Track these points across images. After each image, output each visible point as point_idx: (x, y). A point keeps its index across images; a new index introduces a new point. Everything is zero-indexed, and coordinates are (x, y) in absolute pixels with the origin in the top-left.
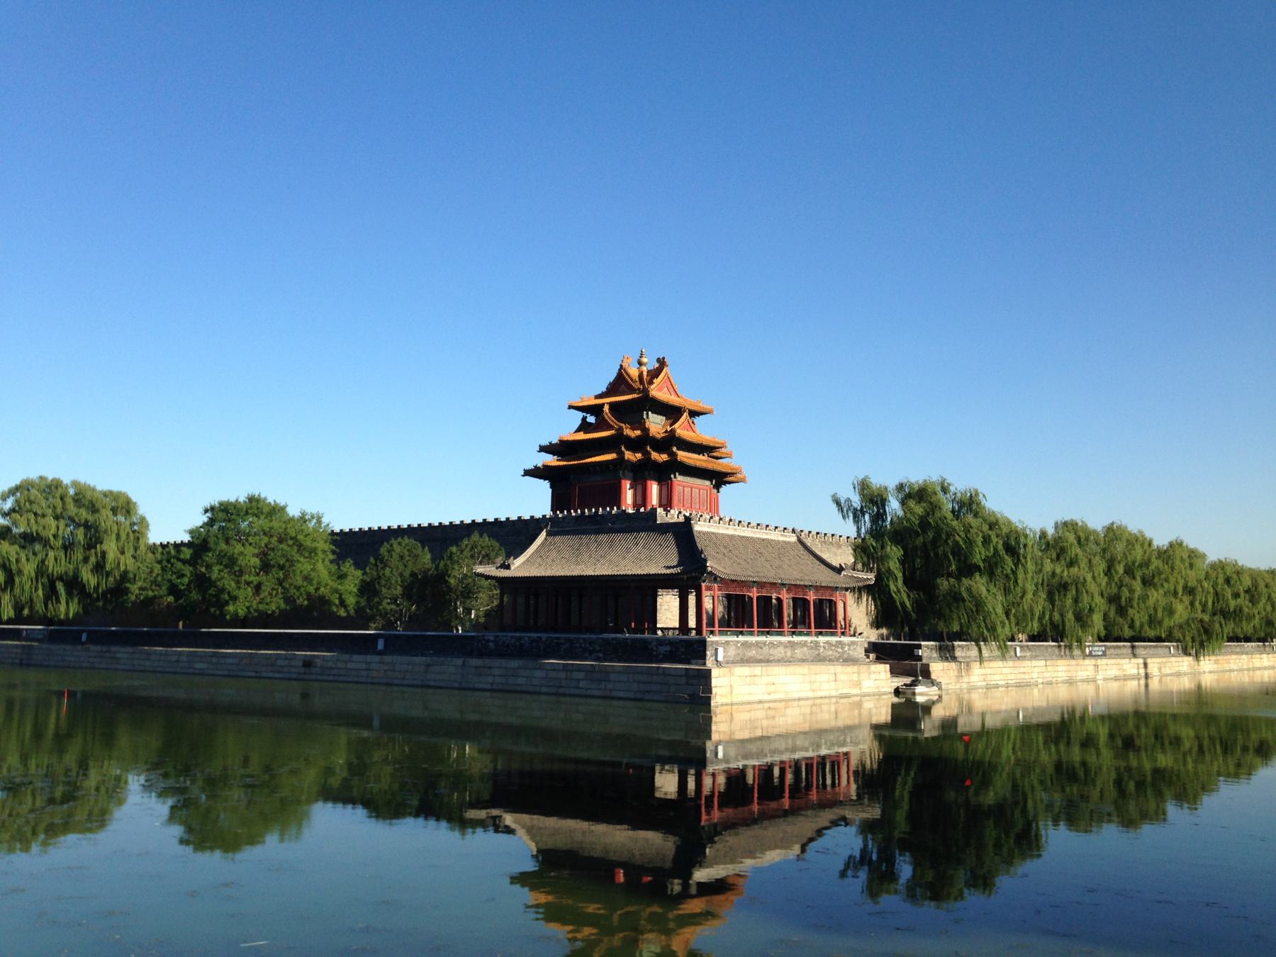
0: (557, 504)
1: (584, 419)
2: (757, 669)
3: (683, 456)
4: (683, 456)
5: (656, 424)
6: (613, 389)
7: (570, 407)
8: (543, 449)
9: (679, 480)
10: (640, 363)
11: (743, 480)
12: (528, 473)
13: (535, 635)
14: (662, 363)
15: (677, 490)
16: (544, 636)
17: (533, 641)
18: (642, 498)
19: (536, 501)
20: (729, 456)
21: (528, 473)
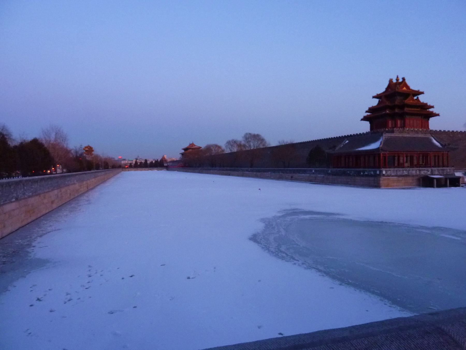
0: (372, 128)
1: (379, 101)
2: (400, 178)
3: (406, 109)
4: (406, 109)
5: (398, 100)
6: (387, 89)
7: (374, 97)
8: (367, 112)
9: (407, 117)
10: (397, 80)
11: (438, 115)
12: (362, 120)
13: (340, 169)
14: (404, 79)
15: (407, 121)
16: (342, 169)
17: (339, 171)
18: (396, 126)
19: (365, 127)
20: (433, 107)
21: (362, 120)
